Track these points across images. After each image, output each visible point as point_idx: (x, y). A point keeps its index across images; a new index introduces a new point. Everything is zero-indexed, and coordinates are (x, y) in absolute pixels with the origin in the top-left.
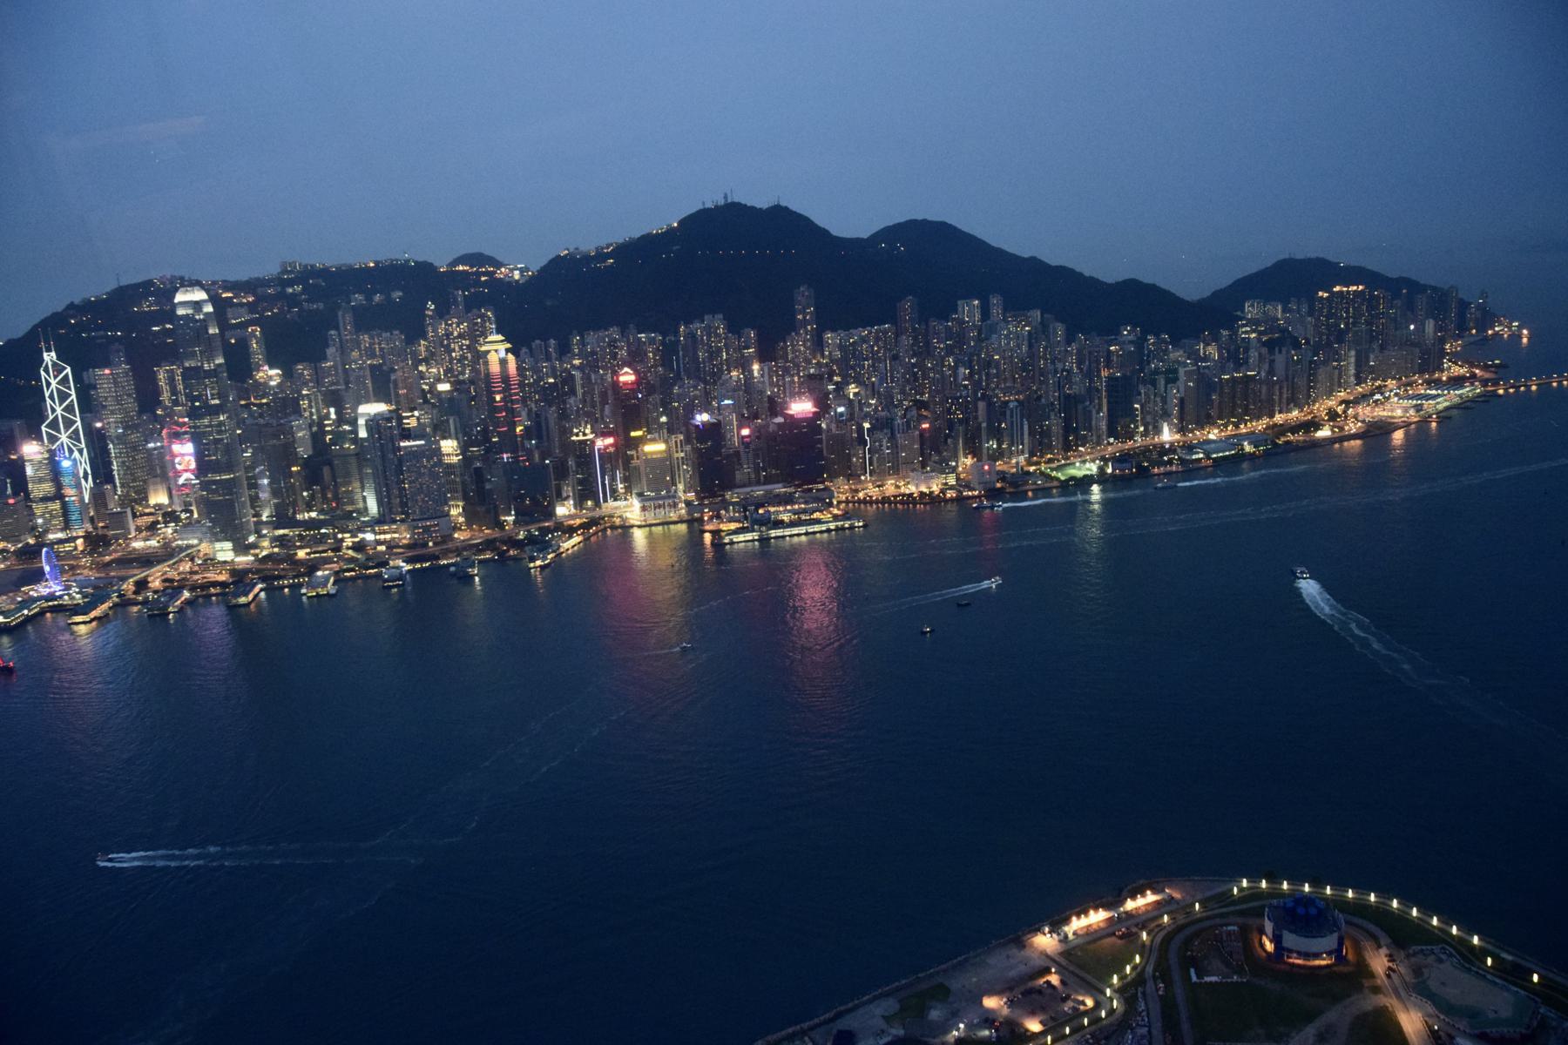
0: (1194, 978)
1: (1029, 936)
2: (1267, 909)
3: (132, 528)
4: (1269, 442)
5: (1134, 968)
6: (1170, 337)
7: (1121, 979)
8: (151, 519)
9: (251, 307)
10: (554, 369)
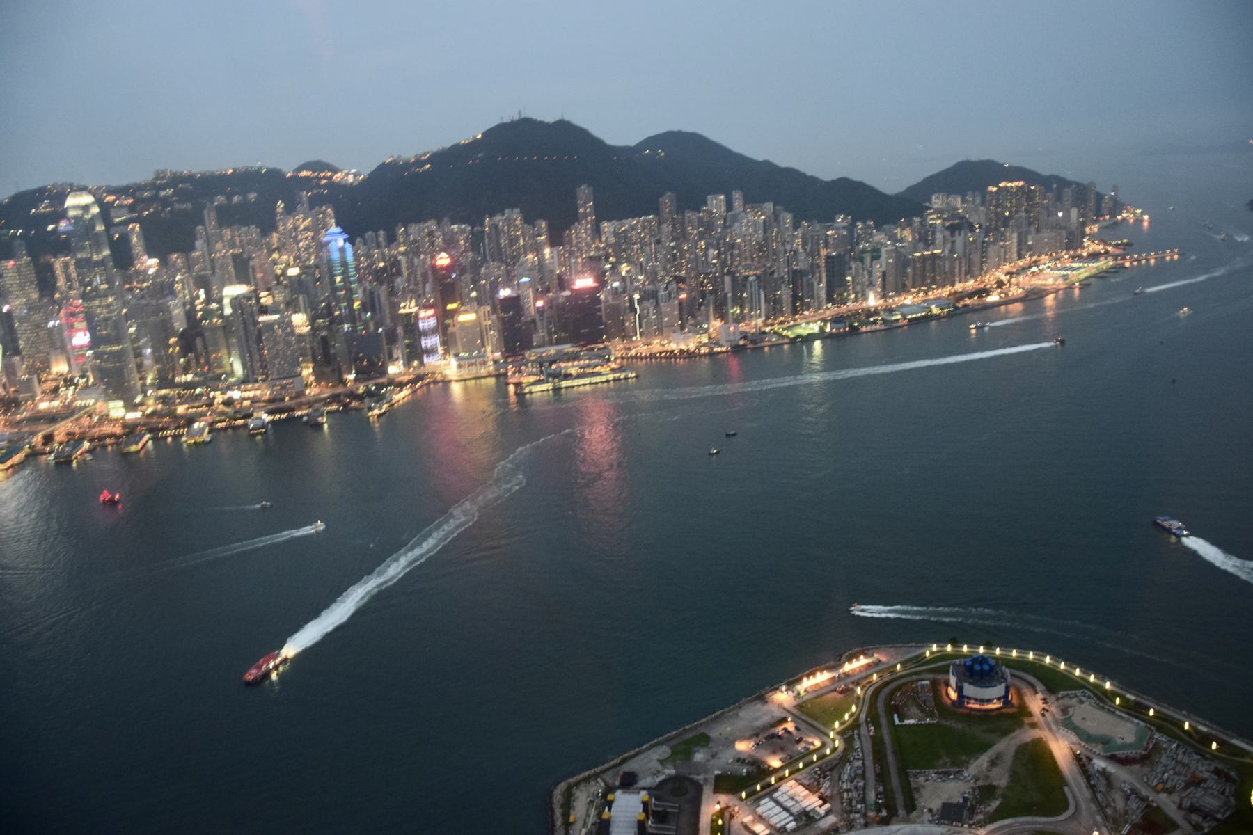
0: (897, 722)
1: (770, 694)
2: (951, 667)
3: (38, 391)
5: (851, 716)
6: (874, 223)
7: (842, 724)
8: (54, 384)
9: (131, 208)
10: (383, 254)
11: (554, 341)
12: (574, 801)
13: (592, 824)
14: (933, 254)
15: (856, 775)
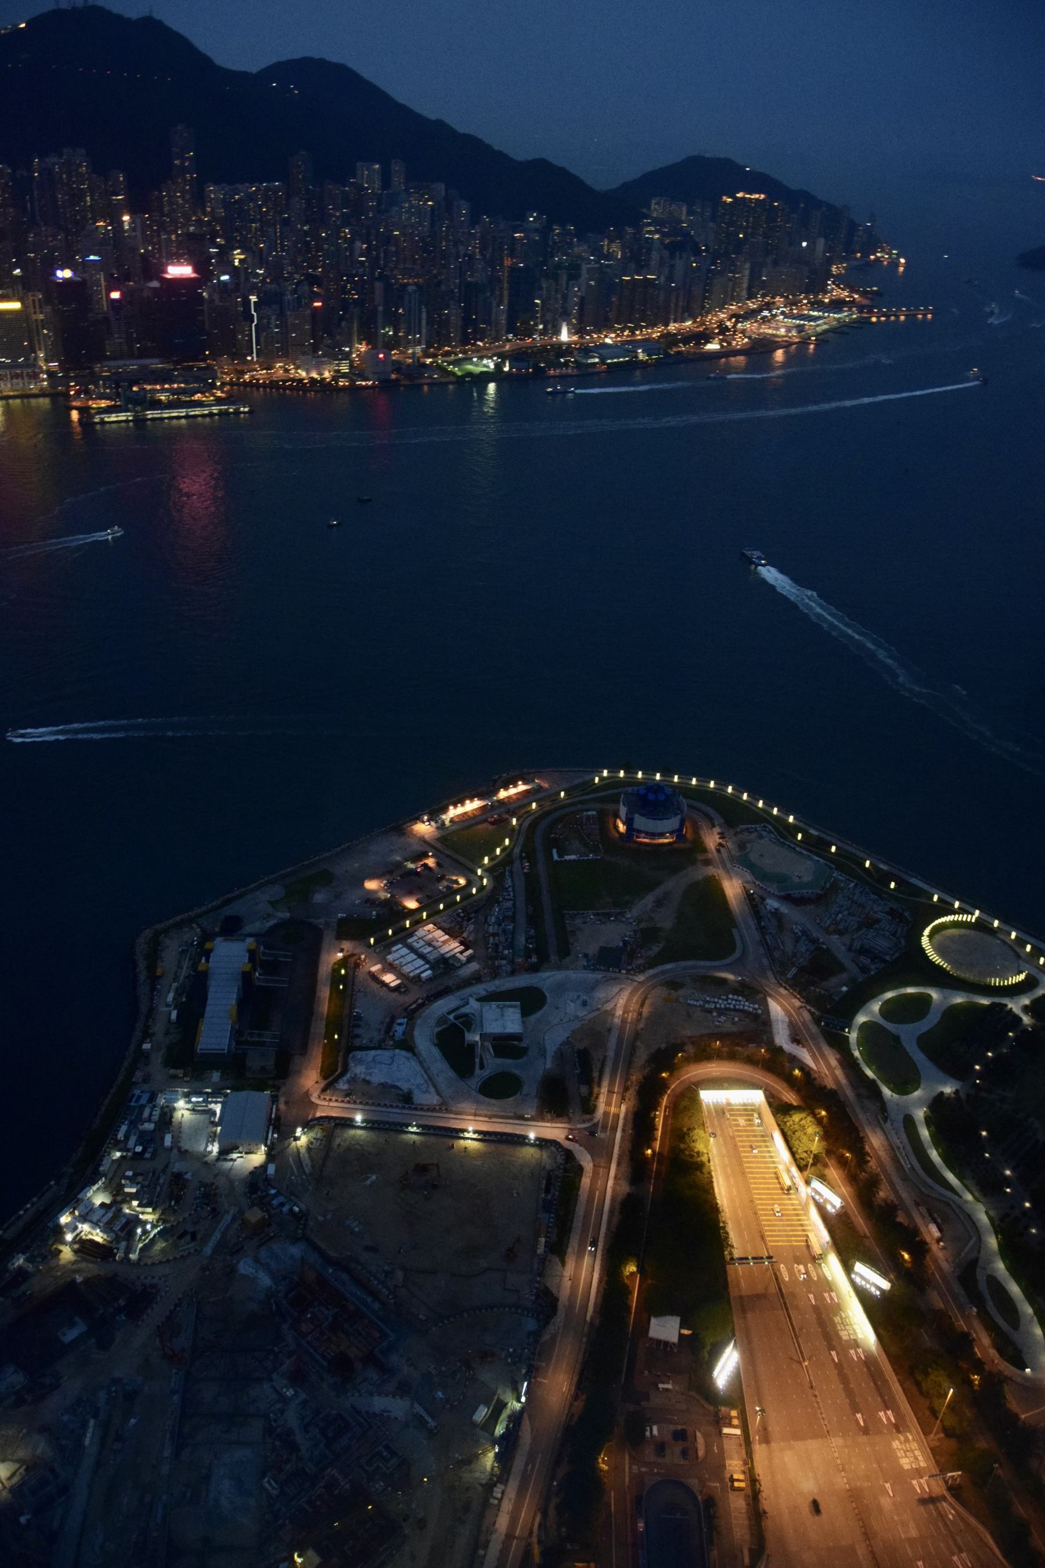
0: (556, 857)
1: (409, 824)
4: (662, 351)
5: (502, 851)
7: (490, 860)
11: (136, 352)
12: (162, 950)
13: (186, 978)
15: (505, 917)
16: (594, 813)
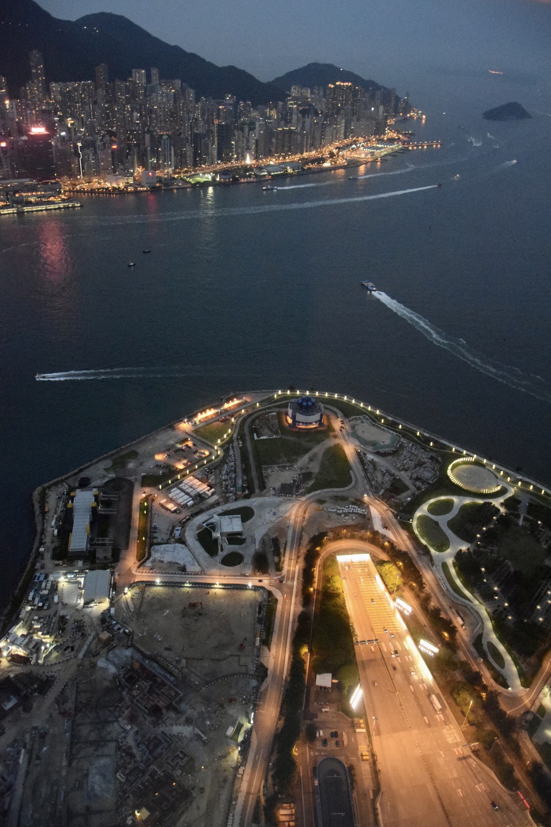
0: (256, 438)
5: (228, 436)
6: (251, 103)
7: (222, 441)
11: (16, 176)
12: (47, 498)
13: (61, 512)
14: (290, 130)
16: (275, 413)
